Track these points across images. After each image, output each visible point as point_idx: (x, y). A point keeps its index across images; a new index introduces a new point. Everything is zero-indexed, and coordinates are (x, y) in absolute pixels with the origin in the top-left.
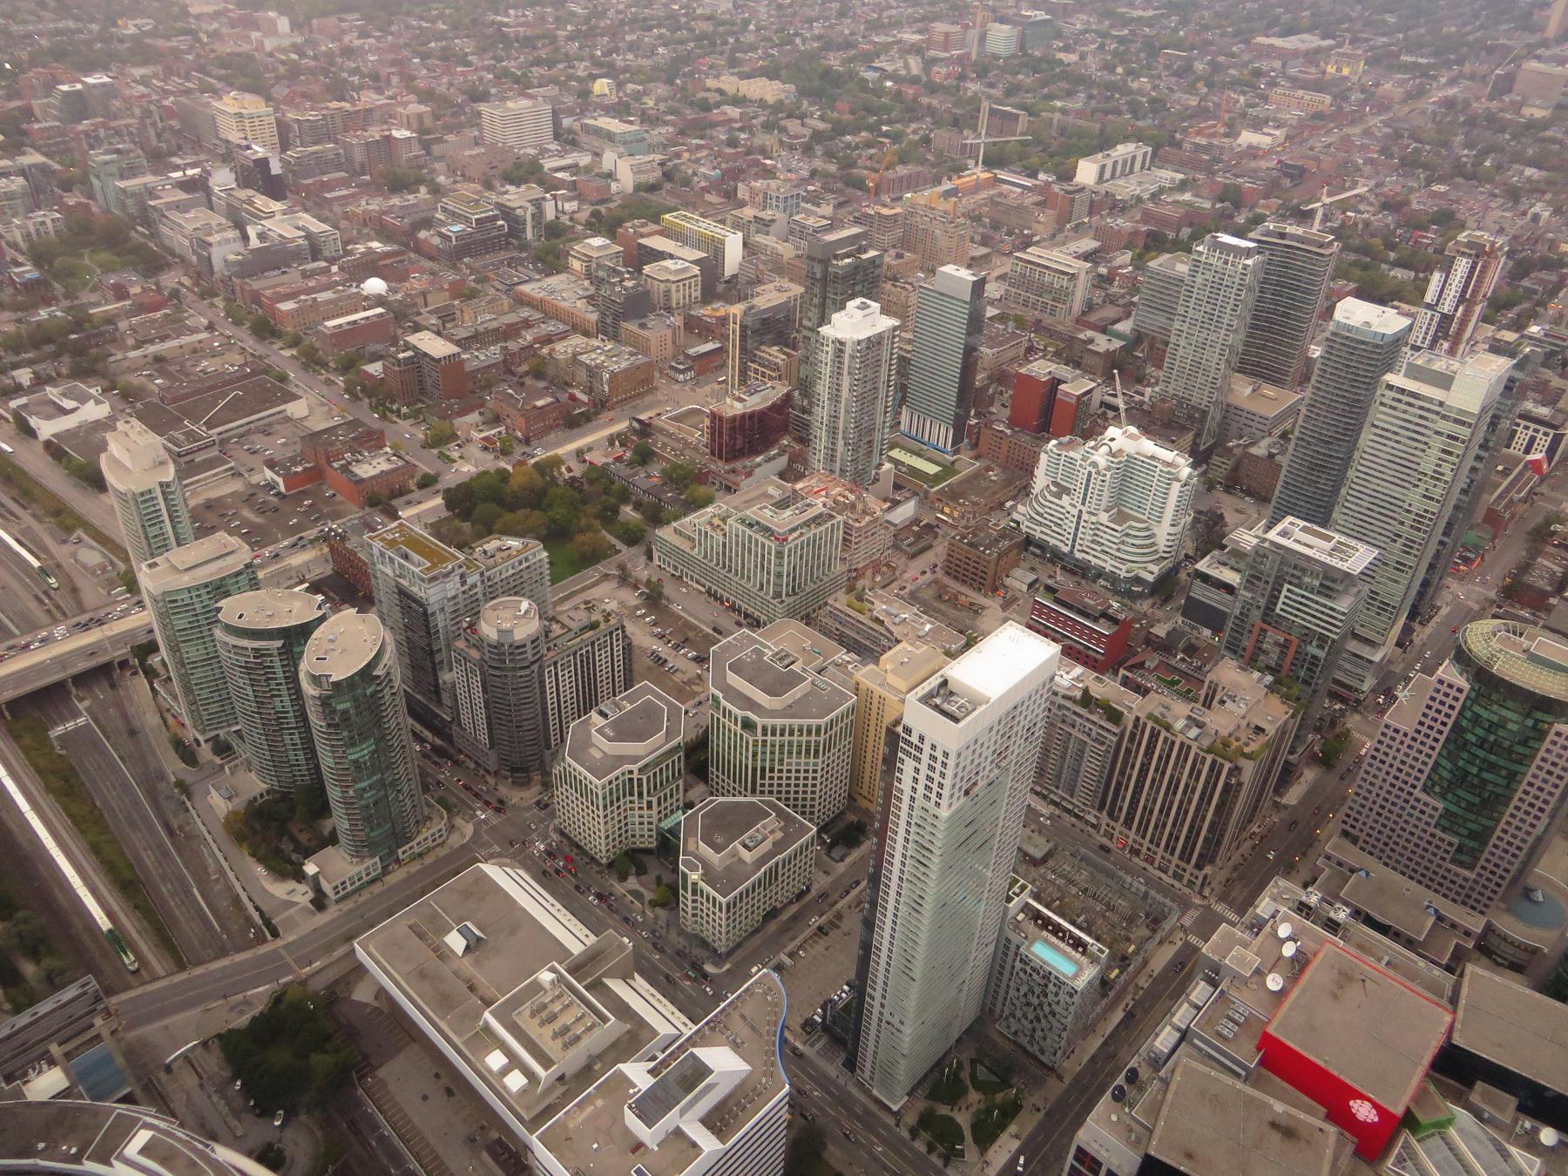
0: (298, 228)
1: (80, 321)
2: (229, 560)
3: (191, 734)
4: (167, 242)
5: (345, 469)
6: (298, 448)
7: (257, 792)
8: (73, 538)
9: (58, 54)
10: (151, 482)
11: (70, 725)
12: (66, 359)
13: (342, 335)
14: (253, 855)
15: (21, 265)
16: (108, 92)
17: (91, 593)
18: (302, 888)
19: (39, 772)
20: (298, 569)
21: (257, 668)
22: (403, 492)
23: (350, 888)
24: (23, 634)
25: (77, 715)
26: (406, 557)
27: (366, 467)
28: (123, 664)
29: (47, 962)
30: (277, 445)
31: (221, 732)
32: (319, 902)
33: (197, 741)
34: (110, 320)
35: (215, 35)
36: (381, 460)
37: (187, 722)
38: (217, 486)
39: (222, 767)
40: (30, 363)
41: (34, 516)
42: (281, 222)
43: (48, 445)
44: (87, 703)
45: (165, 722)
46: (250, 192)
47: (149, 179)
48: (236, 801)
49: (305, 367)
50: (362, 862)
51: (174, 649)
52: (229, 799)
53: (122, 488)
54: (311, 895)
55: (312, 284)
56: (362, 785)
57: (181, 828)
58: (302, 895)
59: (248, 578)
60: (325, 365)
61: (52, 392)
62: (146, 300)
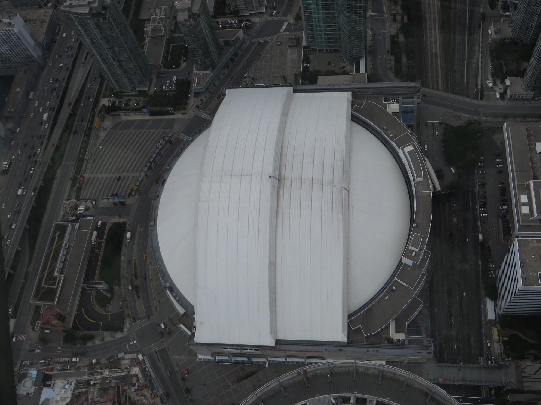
50: (527, 91)
52: (496, 33)
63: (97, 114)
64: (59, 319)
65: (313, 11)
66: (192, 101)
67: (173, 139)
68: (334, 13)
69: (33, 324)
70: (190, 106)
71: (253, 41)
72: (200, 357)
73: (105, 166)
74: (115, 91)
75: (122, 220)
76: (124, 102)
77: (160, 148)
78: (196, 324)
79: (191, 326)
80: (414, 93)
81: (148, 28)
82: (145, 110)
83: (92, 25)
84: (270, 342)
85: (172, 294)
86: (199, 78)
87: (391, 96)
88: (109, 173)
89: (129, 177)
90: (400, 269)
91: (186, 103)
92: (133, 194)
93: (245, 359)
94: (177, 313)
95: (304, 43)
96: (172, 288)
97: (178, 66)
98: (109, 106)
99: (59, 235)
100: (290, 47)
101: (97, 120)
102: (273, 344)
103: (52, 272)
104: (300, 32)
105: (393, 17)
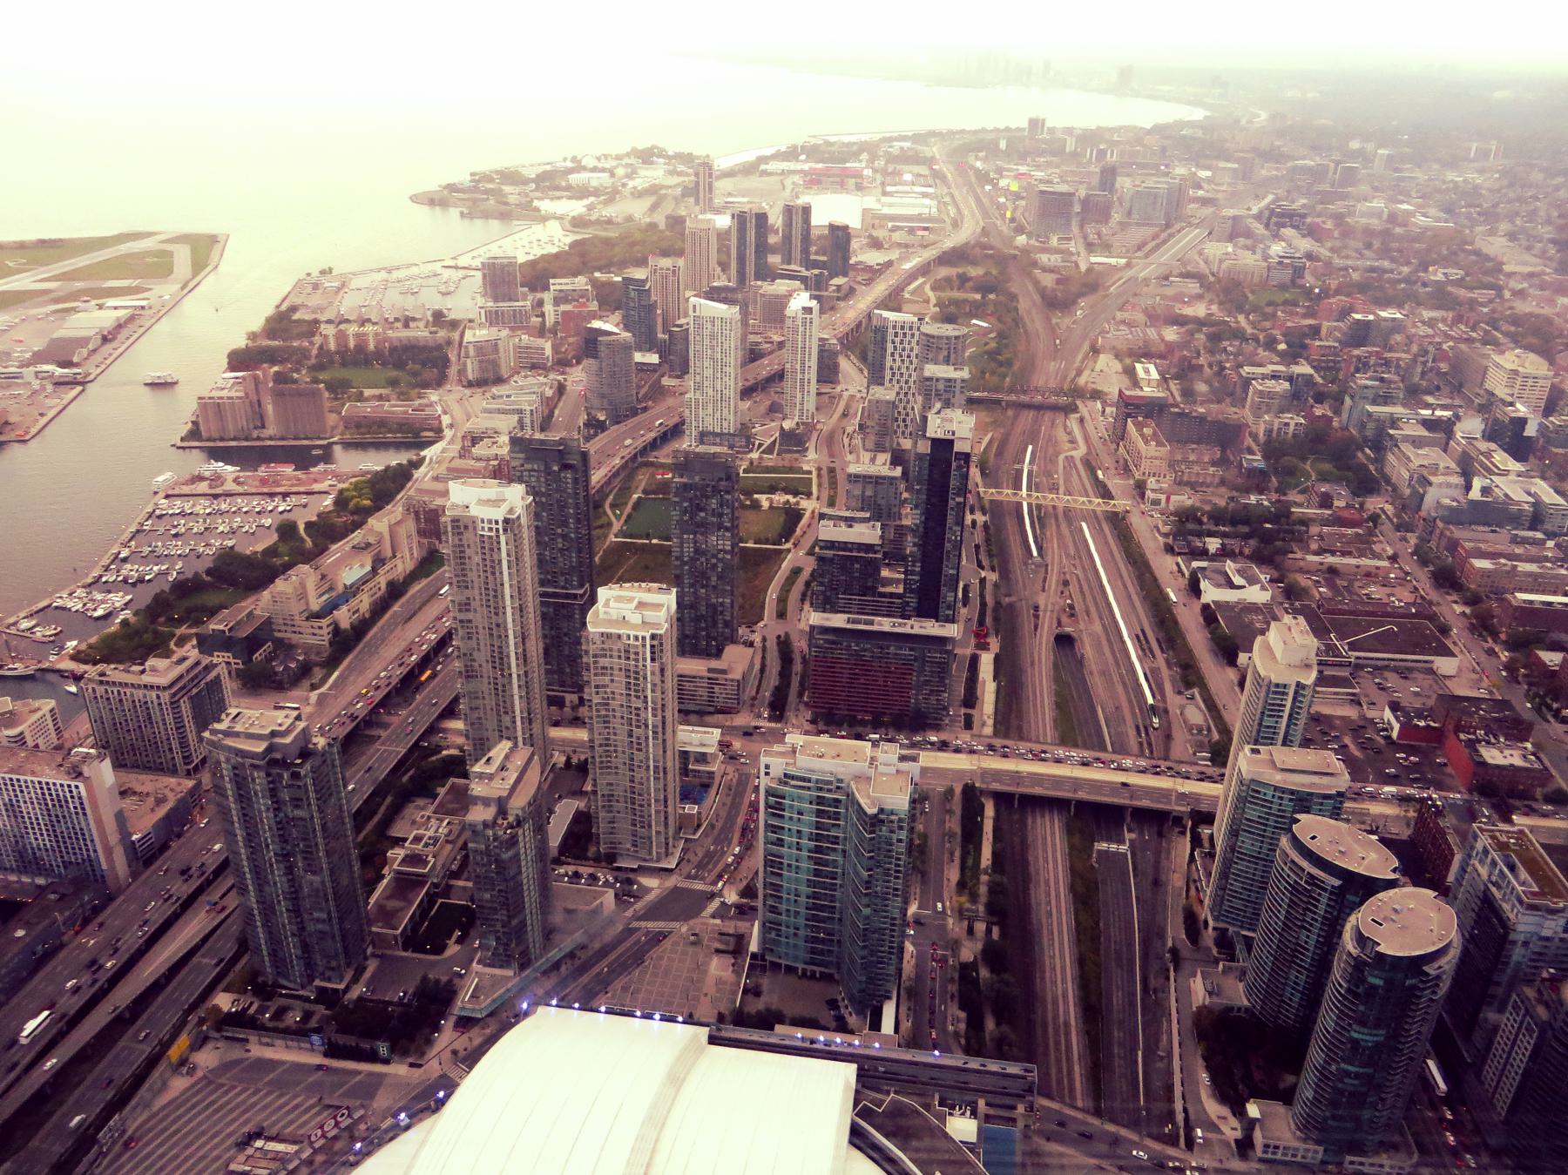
0: (1529, 494)
1: (1282, 514)
2: (1325, 780)
3: (1205, 913)
4: (1388, 470)
5: (1472, 745)
6: (1431, 702)
7: (1237, 1003)
8: (1188, 693)
9: (1363, 287)
10: (1291, 679)
11: (1113, 847)
12: (1252, 542)
13: (1528, 611)
14: (1205, 1058)
15: (1251, 452)
16: (1396, 326)
17: (1181, 745)
18: (1234, 1122)
19: (1072, 869)
20: (1375, 818)
21: (1302, 894)
22: (1525, 795)
23: (1279, 1156)
24: (1114, 752)
25: (1121, 841)
26: (1512, 868)
27: (1495, 752)
28: (1178, 820)
29: (1005, 1028)
30: (1410, 692)
31: (1231, 929)
32: (1244, 1146)
33: (1206, 922)
34: (1305, 522)
35: (1519, 294)
36: (1516, 753)
37: (1207, 902)
38: (1335, 707)
39: (1216, 961)
40: (1224, 535)
41: (1167, 661)
42: (1513, 482)
43: (1206, 607)
44: (1133, 836)
45: (1188, 891)
46: (1493, 446)
47: (1398, 410)
48: (1216, 1000)
49: (1472, 629)
50: (1305, 1140)
51: (1234, 833)
52: (1210, 994)
53: (1263, 673)
54: (1238, 1134)
55: (1519, 550)
56: (1351, 1068)
57: (1155, 991)
58: (1231, 1130)
59: (1334, 806)
60: (1495, 635)
61: (1230, 566)
62: (1345, 514)
63: (189, 1027)
65: (786, 862)
66: (447, 1038)
67: (363, 1127)
68: (833, 887)
70: (434, 1051)
71: (635, 924)
74: (260, 979)
76: (272, 1010)
77: (317, 1145)
80: (1018, 1096)
81: (397, 854)
82: (315, 1038)
83: (259, 781)
86: (479, 982)
87: (958, 1093)
91: (429, 1042)
95: (754, 947)
97: (439, 949)
98: (229, 1014)
100: (718, 951)
101: (183, 1041)
104: (748, 924)
105: (966, 923)
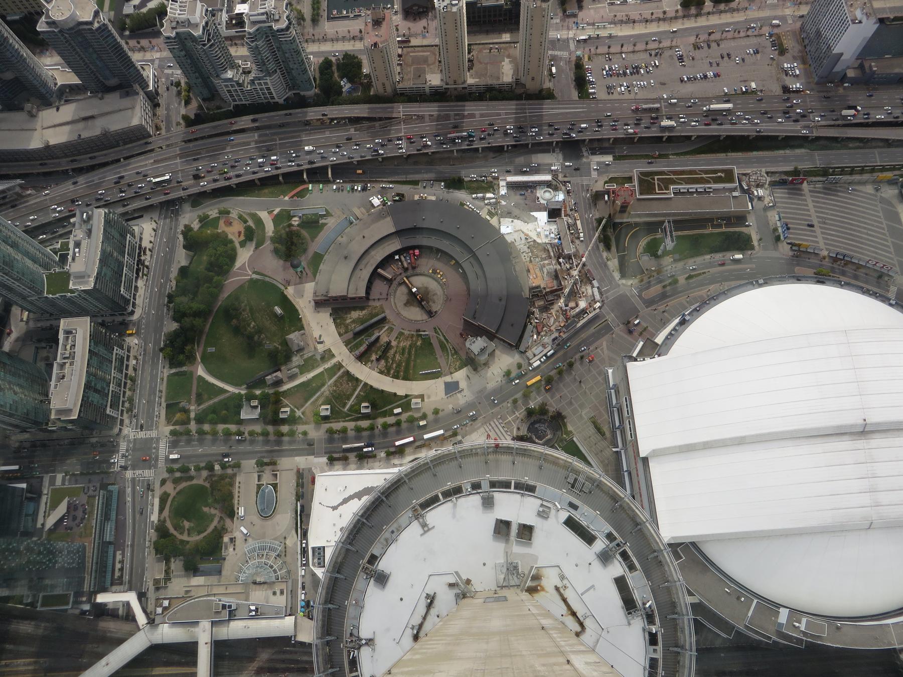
64: (622, 207)
67: (886, 278)
69: (611, 180)
72: (610, 371)
73: (824, 203)
75: (755, 243)
78: (648, 361)
79: (643, 354)
84: (644, 450)
85: (677, 325)
88: (816, 212)
89: (816, 237)
90: (770, 606)
92: (794, 248)
93: (617, 424)
94: (655, 335)
96: (683, 323)
99: (721, 177)
102: (642, 455)
103: (673, 182)
